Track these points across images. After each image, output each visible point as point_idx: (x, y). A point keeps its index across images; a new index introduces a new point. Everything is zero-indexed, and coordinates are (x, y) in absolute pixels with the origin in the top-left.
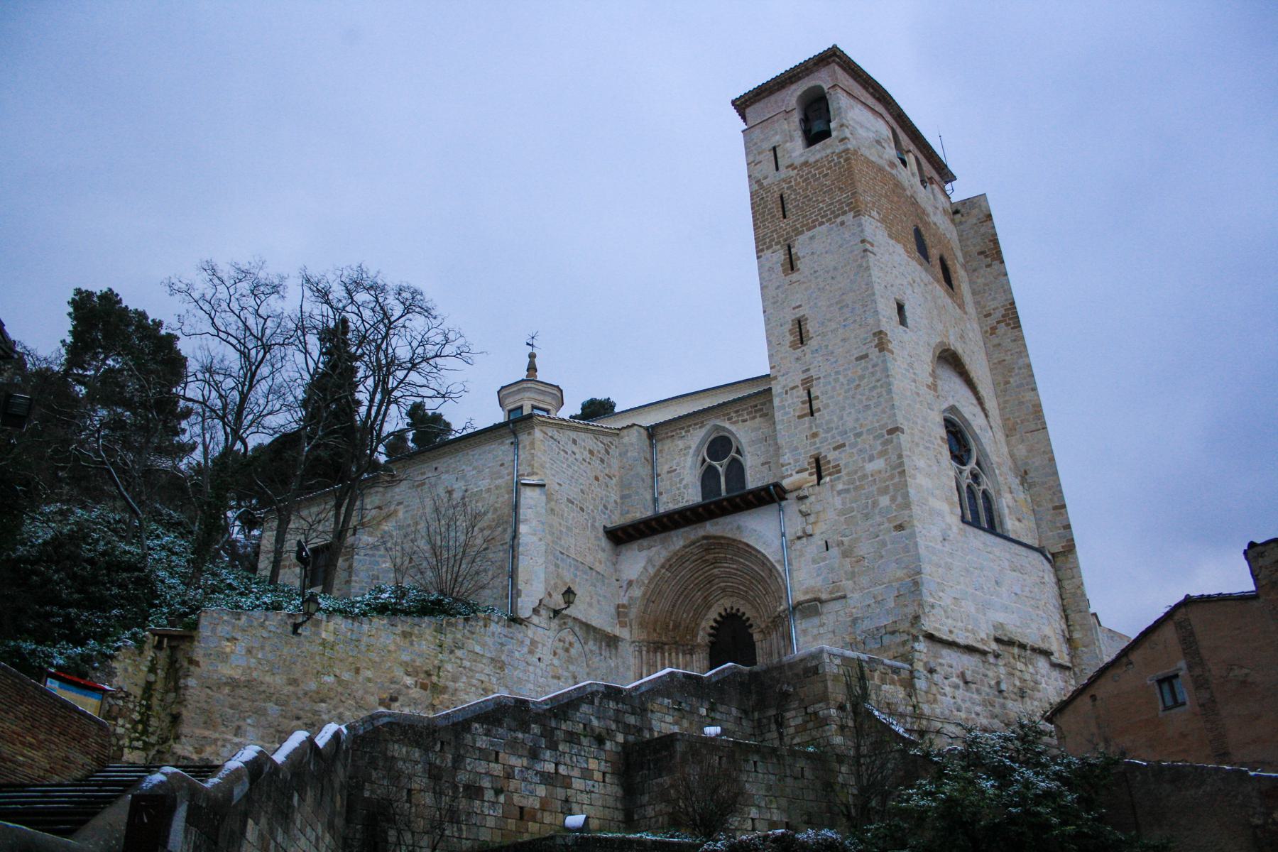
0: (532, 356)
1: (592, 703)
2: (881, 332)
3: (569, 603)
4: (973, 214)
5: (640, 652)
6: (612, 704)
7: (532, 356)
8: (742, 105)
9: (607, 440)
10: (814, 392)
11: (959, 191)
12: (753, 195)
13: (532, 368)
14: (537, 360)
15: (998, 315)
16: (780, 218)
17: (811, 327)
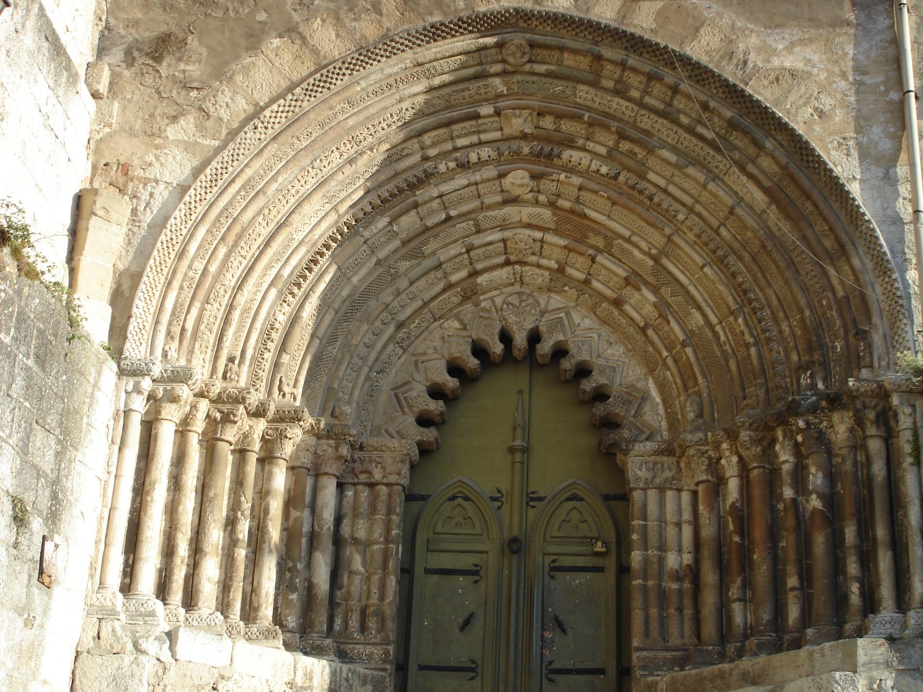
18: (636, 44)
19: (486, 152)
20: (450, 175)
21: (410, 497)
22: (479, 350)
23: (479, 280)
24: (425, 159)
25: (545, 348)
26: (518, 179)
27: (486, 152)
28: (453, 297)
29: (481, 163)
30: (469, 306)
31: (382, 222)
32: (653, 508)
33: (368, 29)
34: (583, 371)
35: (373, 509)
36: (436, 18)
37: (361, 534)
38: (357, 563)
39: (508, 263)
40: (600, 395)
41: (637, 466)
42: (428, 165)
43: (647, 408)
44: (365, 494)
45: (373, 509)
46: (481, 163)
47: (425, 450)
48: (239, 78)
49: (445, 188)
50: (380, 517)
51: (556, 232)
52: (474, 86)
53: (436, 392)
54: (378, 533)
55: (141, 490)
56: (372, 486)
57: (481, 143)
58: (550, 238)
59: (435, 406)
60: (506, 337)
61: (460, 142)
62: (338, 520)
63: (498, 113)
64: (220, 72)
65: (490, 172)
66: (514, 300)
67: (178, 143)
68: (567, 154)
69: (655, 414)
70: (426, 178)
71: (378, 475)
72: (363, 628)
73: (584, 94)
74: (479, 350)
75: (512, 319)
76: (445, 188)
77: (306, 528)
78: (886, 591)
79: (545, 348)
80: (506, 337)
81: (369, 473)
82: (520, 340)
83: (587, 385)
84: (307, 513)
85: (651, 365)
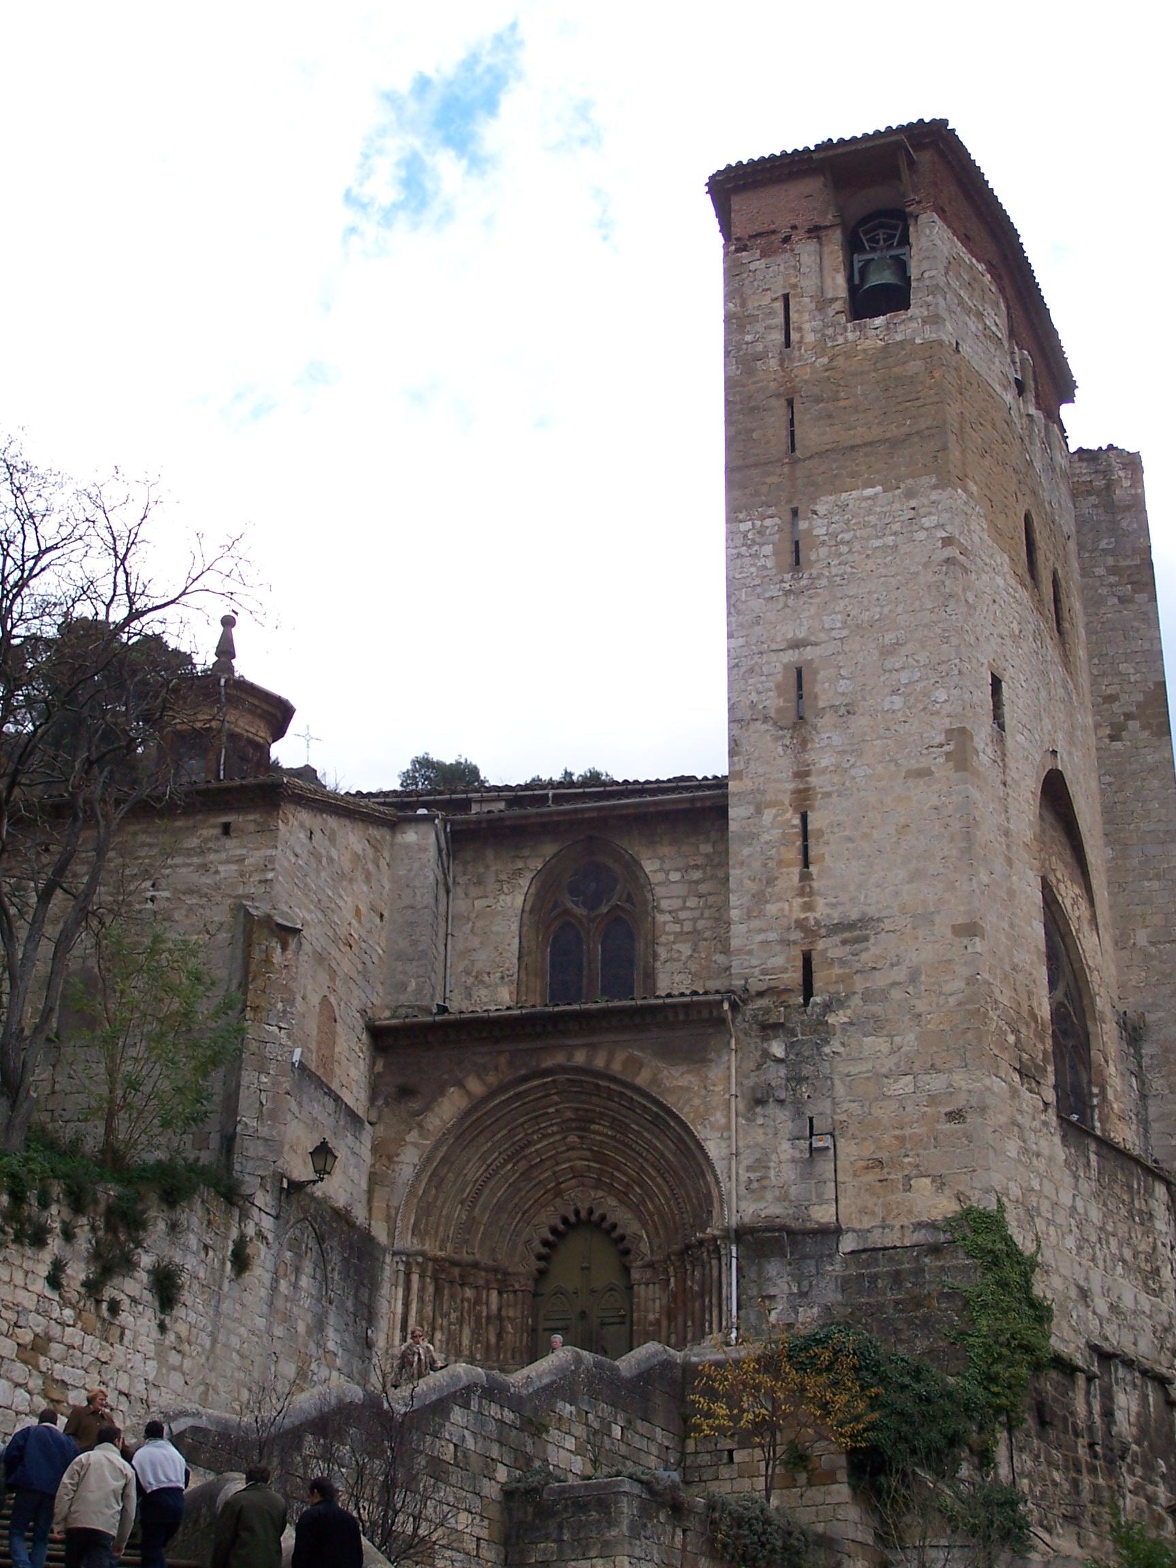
0: (228, 622)
1: (466, 1406)
2: (963, 730)
3: (322, 1172)
4: (1110, 481)
5: (408, 1275)
6: (494, 1410)
7: (228, 622)
8: (732, 187)
9: (375, 832)
10: (815, 821)
11: (1085, 425)
12: (731, 385)
13: (226, 650)
14: (236, 632)
15: (1131, 699)
16: (782, 448)
17: (825, 690)
18: (614, 1079)
19: (555, 1128)
20: (540, 1140)
21: (535, 1295)
22: (565, 1221)
23: (562, 1186)
24: (527, 1135)
25: (595, 1217)
26: (572, 1138)
27: (555, 1128)
28: (549, 1196)
29: (554, 1134)
30: (558, 1199)
31: (509, 1166)
32: (642, 1293)
33: (492, 1079)
34: (614, 1226)
35: (516, 1303)
36: (523, 1072)
37: (511, 1314)
38: (510, 1328)
39: (574, 1177)
40: (622, 1238)
41: (636, 1275)
42: (529, 1138)
43: (641, 1245)
44: (511, 1296)
45: (516, 1303)
46: (554, 1134)
47: (542, 1273)
48: (436, 1109)
49: (538, 1146)
50: (519, 1306)
51: (595, 1161)
52: (544, 1100)
53: (545, 1243)
54: (519, 1314)
55: (406, 1305)
56: (515, 1292)
57: (552, 1125)
58: (592, 1164)
59: (544, 1250)
60: (577, 1213)
61: (543, 1125)
62: (500, 1309)
63: (557, 1111)
64: (427, 1108)
65: (558, 1137)
66: (580, 1195)
67: (412, 1143)
68: (594, 1127)
69: (645, 1247)
70: (530, 1143)
71: (517, 1287)
72: (513, 1358)
73: (595, 1100)
74: (565, 1221)
75: (579, 1204)
76: (538, 1146)
77: (484, 1314)
78: (715, 1326)
79: (595, 1217)
80: (577, 1213)
81: (513, 1286)
82: (583, 1214)
83: (615, 1235)
84: (484, 1307)
85: (644, 1224)
